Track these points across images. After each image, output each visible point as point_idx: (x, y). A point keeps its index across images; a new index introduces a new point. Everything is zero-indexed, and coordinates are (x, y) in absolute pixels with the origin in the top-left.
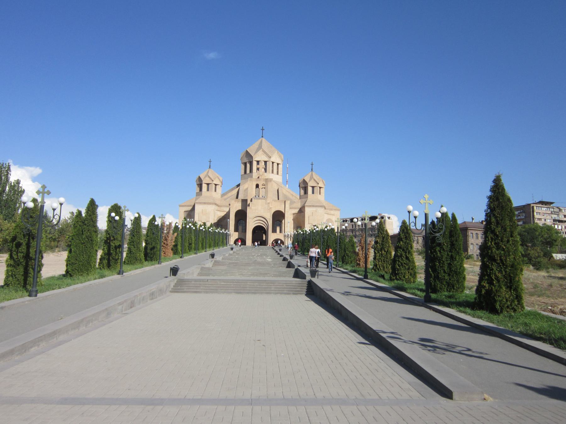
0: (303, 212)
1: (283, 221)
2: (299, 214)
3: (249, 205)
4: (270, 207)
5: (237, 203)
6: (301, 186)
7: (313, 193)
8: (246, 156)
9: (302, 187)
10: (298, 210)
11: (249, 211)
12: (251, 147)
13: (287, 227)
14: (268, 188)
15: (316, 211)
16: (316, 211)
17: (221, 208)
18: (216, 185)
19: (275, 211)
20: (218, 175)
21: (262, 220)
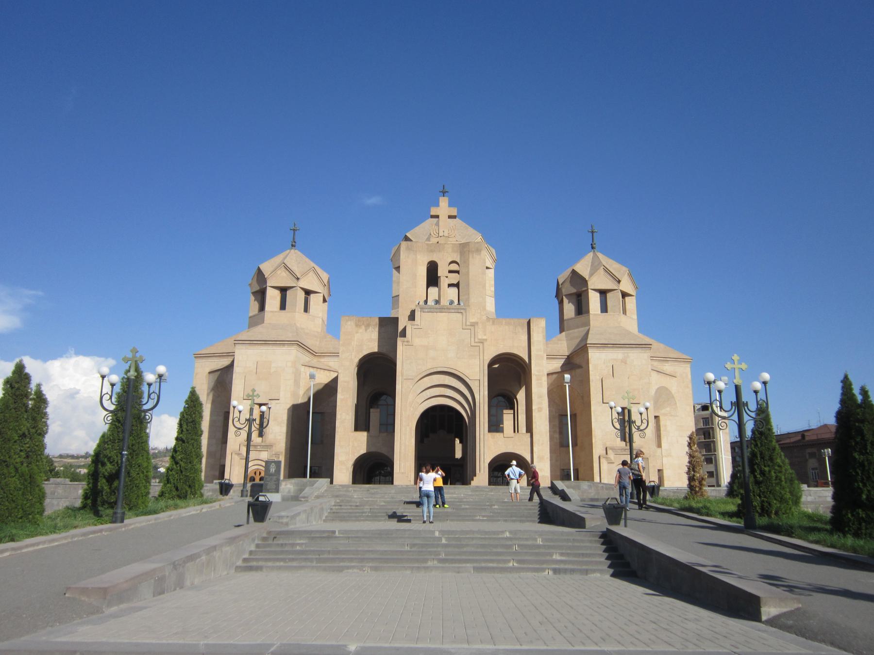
0: (580, 367)
1: (521, 396)
3: (404, 334)
4: (480, 337)
6: (564, 291)
7: (604, 309)
9: (569, 296)
10: (562, 362)
13: (540, 410)
14: (471, 274)
15: (624, 361)
16: (624, 361)
17: (322, 360)
18: (308, 292)
20: (313, 264)
21: (453, 385)
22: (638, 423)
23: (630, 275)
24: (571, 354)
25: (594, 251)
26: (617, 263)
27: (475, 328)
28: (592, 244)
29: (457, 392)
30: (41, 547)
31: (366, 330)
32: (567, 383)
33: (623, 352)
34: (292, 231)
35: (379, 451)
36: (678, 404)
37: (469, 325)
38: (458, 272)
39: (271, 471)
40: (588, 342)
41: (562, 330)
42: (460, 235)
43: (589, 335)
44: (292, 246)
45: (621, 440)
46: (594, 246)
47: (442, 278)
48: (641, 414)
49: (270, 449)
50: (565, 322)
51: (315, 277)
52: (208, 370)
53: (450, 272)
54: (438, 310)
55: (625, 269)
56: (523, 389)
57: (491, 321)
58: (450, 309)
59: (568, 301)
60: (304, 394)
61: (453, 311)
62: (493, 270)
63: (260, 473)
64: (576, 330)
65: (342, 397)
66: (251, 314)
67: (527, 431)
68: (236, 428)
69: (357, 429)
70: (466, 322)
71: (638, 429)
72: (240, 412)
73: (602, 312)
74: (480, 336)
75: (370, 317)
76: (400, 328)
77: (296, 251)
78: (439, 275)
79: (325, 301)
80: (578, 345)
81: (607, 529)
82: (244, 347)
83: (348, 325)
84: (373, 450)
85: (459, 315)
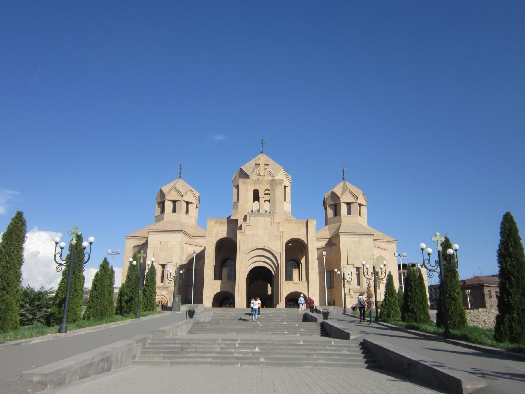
0: (335, 245)
1: (303, 261)
2: (328, 248)
3: (240, 228)
4: (281, 230)
5: (218, 225)
7: (349, 213)
8: (240, 176)
9: (330, 206)
10: (326, 242)
11: (240, 236)
12: (247, 165)
13: (313, 269)
15: (359, 242)
16: (359, 242)
18: (188, 203)
19: (289, 239)
20: (191, 188)
21: (267, 256)
22: (348, 279)
23: (364, 195)
24: (330, 238)
25: (344, 181)
26: (356, 188)
27: (278, 226)
28: (343, 177)
29: (268, 259)
30: (123, 324)
31: (220, 226)
32: (325, 256)
33: (358, 237)
34: (179, 169)
35: (227, 290)
36: (389, 265)
37: (275, 224)
38: (269, 194)
39: (176, 300)
40: (340, 232)
41: (326, 225)
42: (271, 168)
43: (341, 228)
44: (179, 177)
45: (358, 285)
46: (344, 178)
47: (261, 198)
48: (349, 275)
49: (167, 289)
50: (328, 220)
51: (192, 194)
52: (133, 246)
53: (265, 194)
54: (259, 216)
55: (360, 191)
56: (305, 257)
57: (287, 221)
58: (265, 215)
59: (329, 208)
60: (186, 259)
61: (267, 216)
62: (290, 188)
63: (162, 303)
64: (334, 225)
65: (208, 262)
66: (156, 215)
67: (306, 281)
68: (169, 280)
69: (215, 278)
70: (273, 223)
71: (347, 282)
72: (171, 273)
73: (348, 215)
74: (281, 229)
75: (223, 219)
76: (239, 225)
77: (181, 180)
78: (259, 197)
79: (197, 207)
80: (335, 233)
81: (323, 321)
82: (153, 233)
83: (211, 223)
84: (224, 290)
85: (270, 219)
